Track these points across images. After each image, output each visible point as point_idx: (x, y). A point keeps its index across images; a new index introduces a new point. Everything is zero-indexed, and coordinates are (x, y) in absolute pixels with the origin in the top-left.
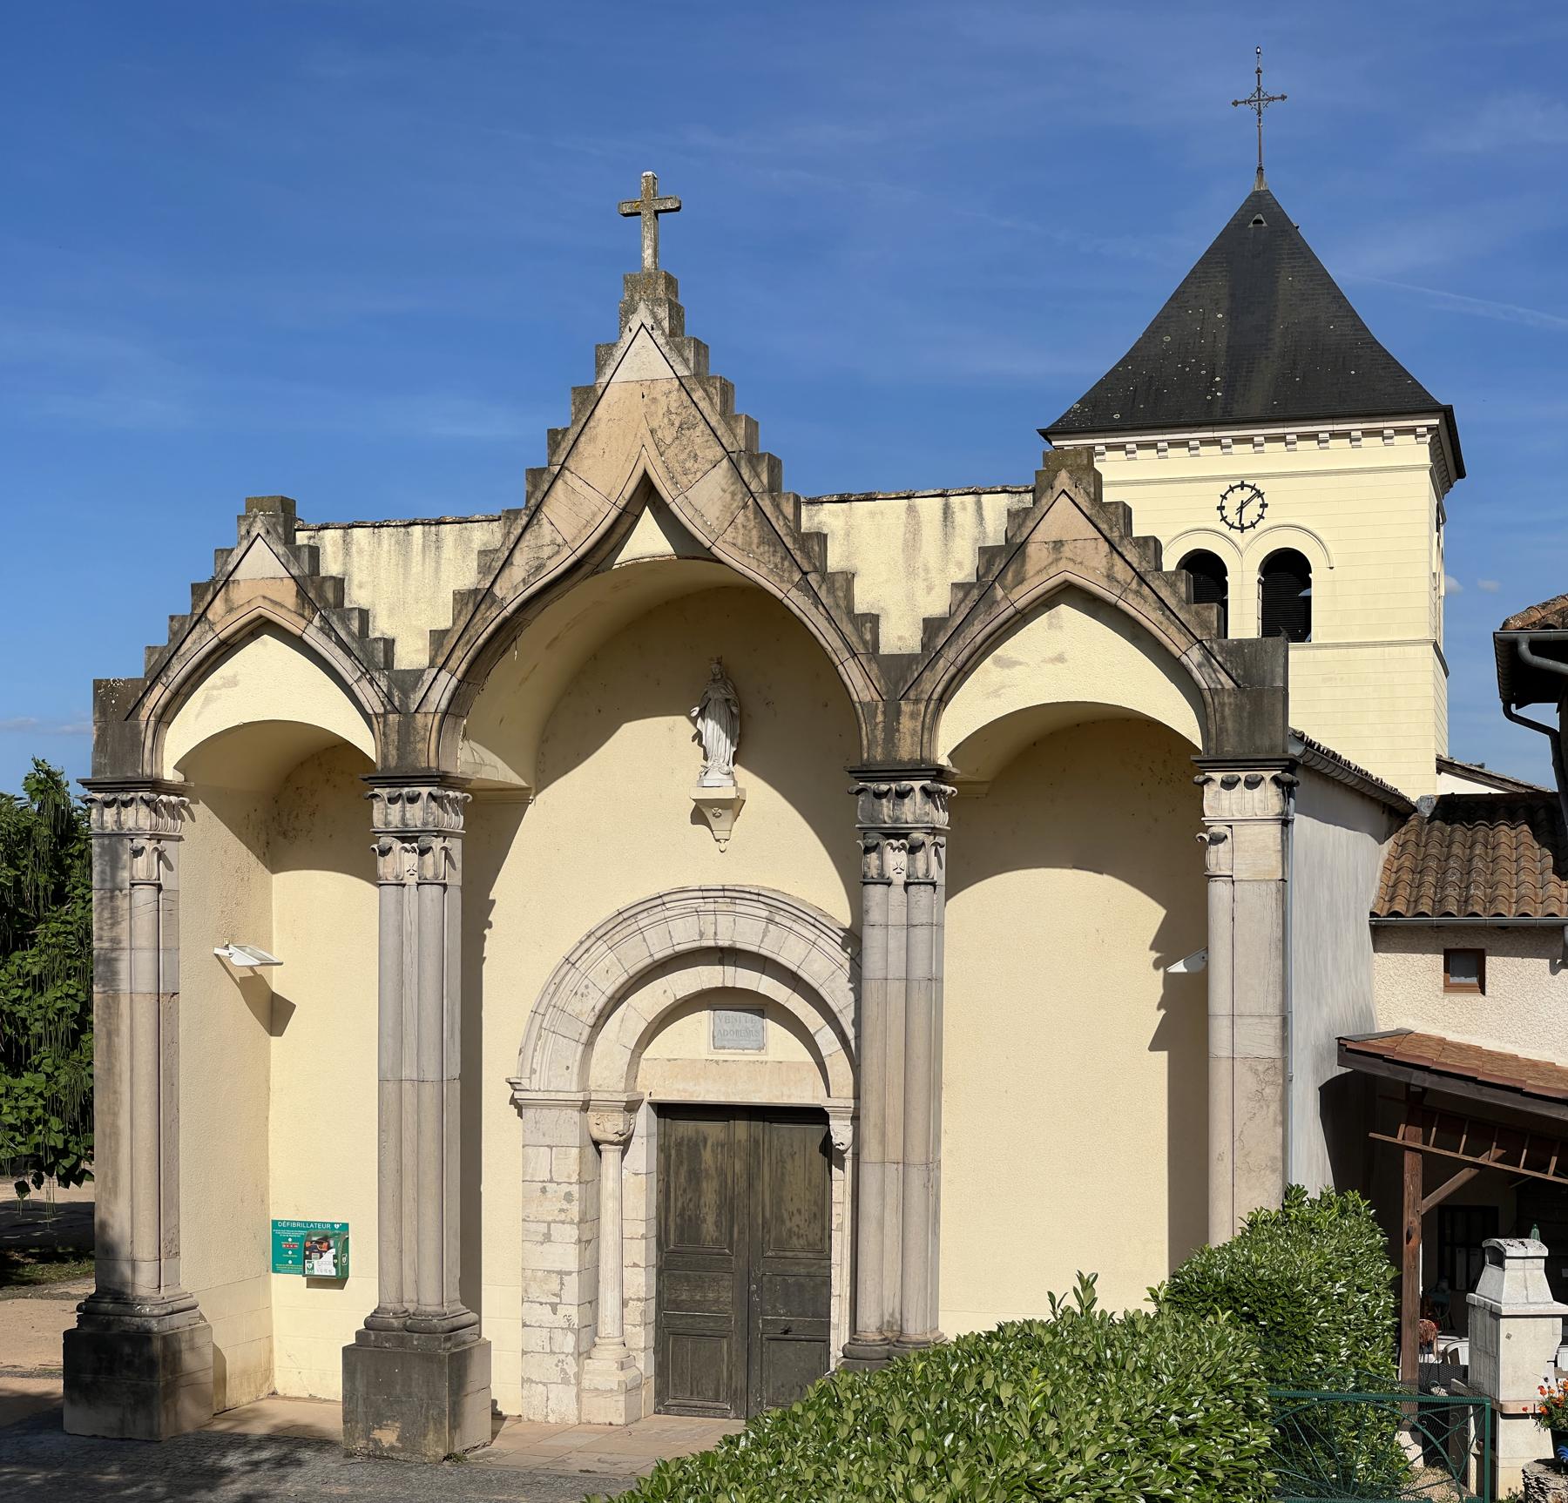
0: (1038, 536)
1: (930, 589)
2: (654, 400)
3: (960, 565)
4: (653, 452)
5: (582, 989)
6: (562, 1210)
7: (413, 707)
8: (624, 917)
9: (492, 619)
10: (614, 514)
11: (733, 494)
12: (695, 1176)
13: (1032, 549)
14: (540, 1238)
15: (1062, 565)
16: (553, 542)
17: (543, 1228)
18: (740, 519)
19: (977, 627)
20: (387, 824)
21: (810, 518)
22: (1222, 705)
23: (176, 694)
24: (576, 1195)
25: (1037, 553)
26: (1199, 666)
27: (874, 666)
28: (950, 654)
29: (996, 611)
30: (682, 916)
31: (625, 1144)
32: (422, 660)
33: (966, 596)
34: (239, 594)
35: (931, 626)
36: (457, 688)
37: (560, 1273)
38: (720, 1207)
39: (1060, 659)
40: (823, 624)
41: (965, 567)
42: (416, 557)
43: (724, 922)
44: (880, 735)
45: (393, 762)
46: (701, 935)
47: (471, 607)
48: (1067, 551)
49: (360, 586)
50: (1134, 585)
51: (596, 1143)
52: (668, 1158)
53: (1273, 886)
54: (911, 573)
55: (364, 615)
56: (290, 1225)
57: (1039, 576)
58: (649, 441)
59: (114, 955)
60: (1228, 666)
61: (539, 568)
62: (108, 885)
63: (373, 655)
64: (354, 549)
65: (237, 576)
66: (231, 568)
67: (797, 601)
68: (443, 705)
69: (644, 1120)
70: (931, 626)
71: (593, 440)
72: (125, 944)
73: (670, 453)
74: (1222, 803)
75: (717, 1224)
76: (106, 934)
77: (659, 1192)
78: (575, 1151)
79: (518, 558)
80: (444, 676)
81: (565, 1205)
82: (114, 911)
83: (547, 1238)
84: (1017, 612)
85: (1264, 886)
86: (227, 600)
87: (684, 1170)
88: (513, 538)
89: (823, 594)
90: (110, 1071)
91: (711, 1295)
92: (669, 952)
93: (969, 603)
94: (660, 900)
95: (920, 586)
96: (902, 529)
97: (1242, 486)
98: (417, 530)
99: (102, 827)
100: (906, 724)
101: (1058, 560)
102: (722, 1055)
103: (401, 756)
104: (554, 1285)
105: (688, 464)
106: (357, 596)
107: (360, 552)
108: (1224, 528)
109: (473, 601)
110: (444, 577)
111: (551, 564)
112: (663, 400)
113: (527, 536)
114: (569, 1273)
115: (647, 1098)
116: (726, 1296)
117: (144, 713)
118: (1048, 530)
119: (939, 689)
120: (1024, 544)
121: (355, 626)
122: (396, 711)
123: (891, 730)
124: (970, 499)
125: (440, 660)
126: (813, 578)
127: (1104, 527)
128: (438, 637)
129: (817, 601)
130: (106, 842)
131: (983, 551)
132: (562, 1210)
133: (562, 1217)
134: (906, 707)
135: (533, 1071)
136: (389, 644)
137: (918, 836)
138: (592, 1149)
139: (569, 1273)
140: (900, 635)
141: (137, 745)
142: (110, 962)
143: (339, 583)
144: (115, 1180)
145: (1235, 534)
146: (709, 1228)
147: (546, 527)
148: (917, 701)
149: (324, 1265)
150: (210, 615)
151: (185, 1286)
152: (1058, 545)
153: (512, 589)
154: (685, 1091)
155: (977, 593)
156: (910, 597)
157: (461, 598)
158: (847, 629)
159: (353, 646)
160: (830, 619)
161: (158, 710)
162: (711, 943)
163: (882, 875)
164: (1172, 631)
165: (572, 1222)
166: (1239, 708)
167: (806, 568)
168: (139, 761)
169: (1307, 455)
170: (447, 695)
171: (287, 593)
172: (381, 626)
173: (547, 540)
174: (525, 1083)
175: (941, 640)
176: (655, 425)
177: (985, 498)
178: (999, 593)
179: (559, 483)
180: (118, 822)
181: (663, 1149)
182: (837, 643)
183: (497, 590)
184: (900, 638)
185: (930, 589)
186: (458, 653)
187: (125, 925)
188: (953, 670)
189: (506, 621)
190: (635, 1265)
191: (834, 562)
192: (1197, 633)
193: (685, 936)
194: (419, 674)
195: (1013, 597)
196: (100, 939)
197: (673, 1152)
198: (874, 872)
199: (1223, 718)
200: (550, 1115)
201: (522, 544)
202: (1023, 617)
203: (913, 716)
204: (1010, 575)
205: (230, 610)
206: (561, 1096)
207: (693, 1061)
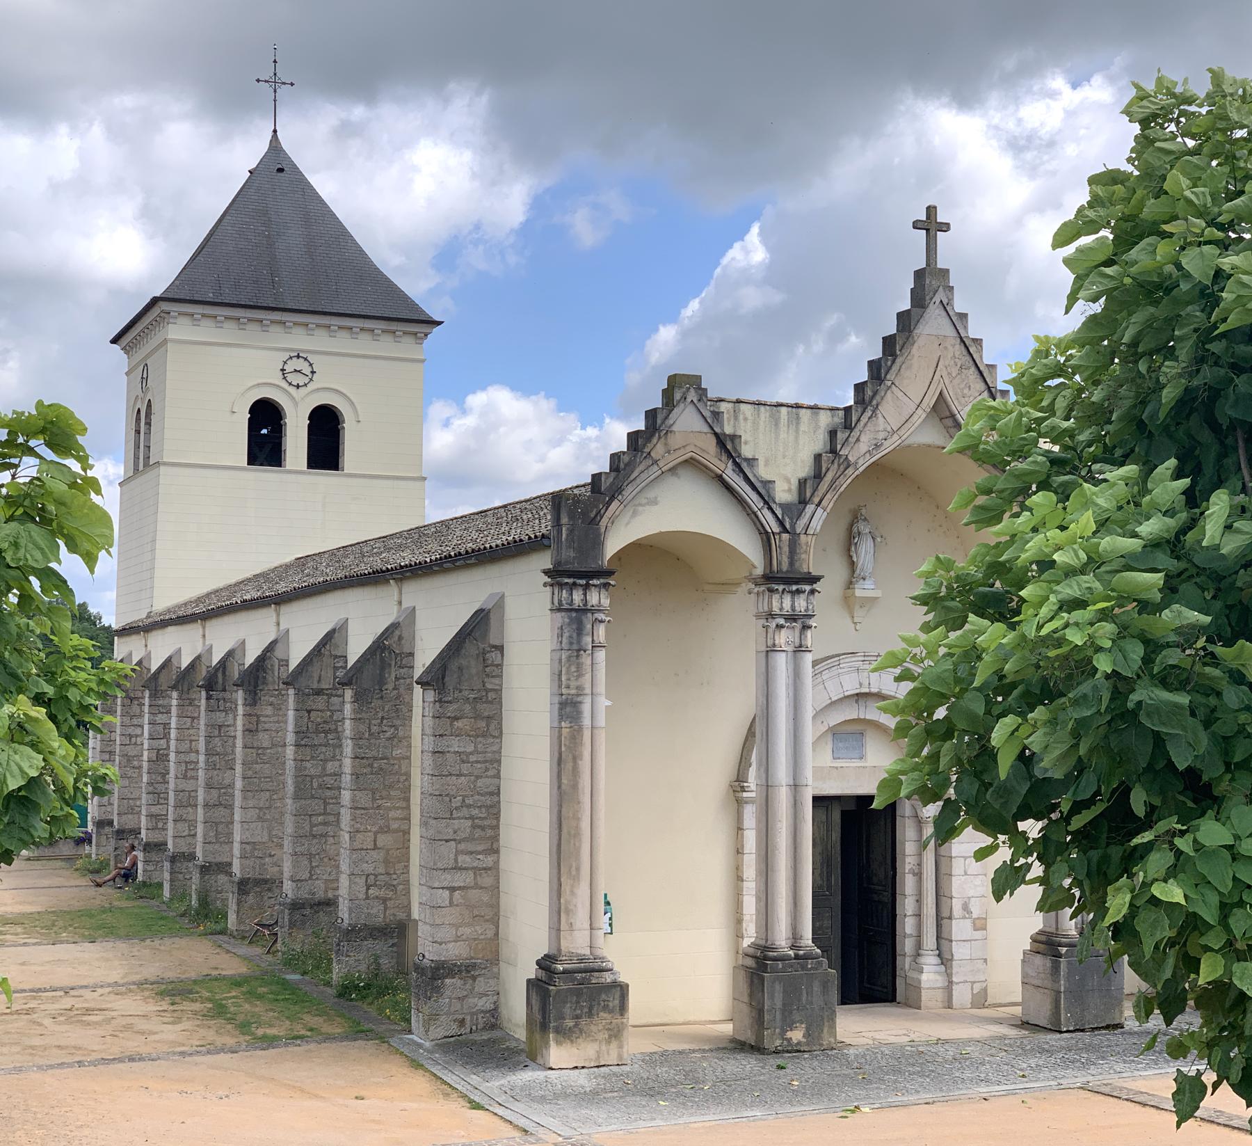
20: (781, 609)
45: (785, 567)
46: (861, 684)
59: (579, 699)
61: (877, 446)
62: (575, 647)
64: (741, 417)
71: (910, 367)
72: (588, 691)
73: (956, 381)
76: (573, 684)
80: (820, 510)
86: (666, 444)
98: (784, 410)
99: (571, 603)
102: (838, 764)
103: (791, 563)
105: (966, 391)
107: (746, 419)
110: (801, 442)
112: (950, 348)
122: (785, 530)
125: (816, 500)
130: (574, 615)
144: (578, 869)
147: (881, 419)
159: (758, 485)
162: (867, 690)
169: (342, 342)
171: (710, 444)
173: (881, 428)
180: (585, 602)
186: (829, 496)
187: (588, 676)
196: (568, 687)
207: (823, 768)
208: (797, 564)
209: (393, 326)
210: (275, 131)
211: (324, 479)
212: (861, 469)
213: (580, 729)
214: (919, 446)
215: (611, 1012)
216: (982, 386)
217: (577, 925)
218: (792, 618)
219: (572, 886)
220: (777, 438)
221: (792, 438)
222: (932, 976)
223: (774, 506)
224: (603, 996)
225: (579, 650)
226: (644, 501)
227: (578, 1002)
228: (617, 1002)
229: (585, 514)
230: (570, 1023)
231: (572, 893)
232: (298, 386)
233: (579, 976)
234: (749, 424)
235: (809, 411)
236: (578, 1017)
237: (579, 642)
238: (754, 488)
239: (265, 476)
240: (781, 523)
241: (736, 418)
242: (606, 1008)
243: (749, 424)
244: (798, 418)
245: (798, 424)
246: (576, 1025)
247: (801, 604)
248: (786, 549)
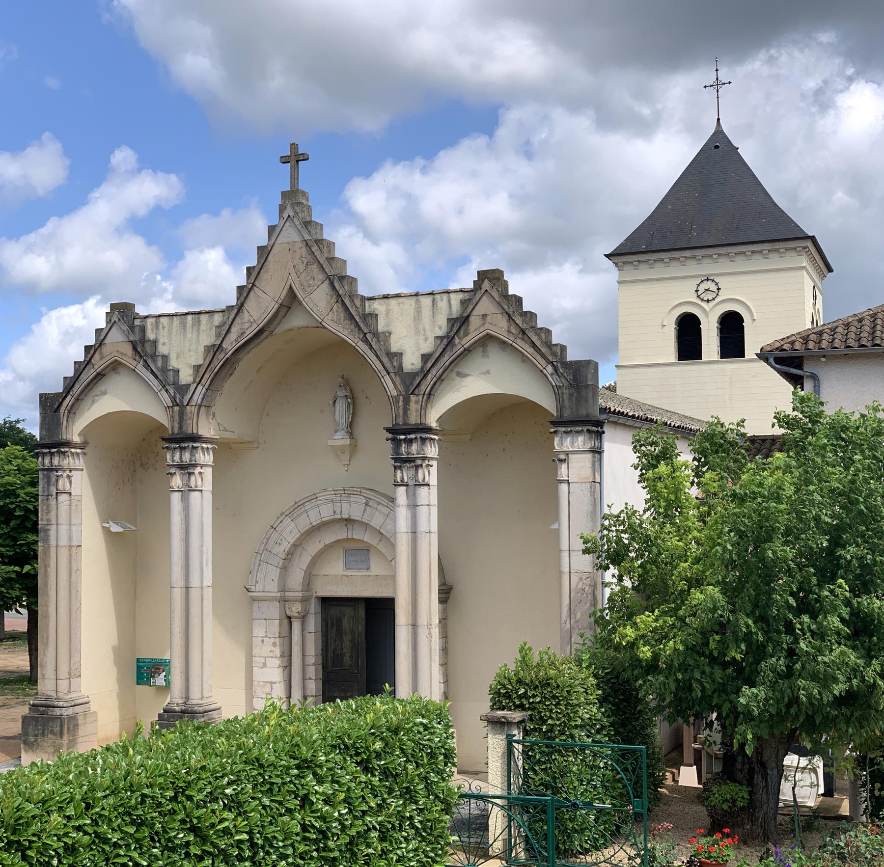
0: (475, 312)
1: (426, 339)
2: (295, 251)
3: (440, 327)
4: (294, 275)
5: (279, 541)
6: (271, 651)
7: (185, 403)
8: (298, 505)
9: (221, 357)
10: (276, 307)
11: (332, 296)
12: (340, 633)
13: (472, 319)
14: (261, 665)
15: (487, 326)
16: (249, 321)
17: (263, 660)
18: (335, 308)
19: (446, 357)
21: (370, 306)
22: (563, 394)
23: (77, 400)
24: (278, 643)
25: (474, 321)
26: (552, 375)
27: (398, 378)
28: (434, 371)
29: (455, 349)
30: (325, 504)
31: (303, 618)
32: (190, 379)
33: (442, 341)
34: (106, 350)
35: (425, 358)
36: (205, 393)
37: (271, 683)
40: (374, 358)
41: (441, 327)
42: (189, 329)
43: (345, 505)
44: (401, 411)
45: (176, 431)
46: (334, 512)
47: (211, 354)
48: (488, 319)
49: (164, 344)
50: (520, 336)
51: (289, 618)
52: (327, 625)
53: (588, 485)
54: (417, 332)
55: (165, 358)
56: (145, 661)
57: (475, 330)
58: (292, 271)
60: (565, 374)
61: (242, 334)
62: (46, 493)
63: (165, 376)
65: (106, 341)
66: (102, 338)
67: (362, 347)
68: (199, 402)
69: (314, 607)
70: (425, 358)
71: (267, 271)
72: (54, 521)
73: (302, 277)
74: (563, 443)
76: (45, 518)
77: (323, 642)
78: (277, 622)
79: (233, 330)
81: (273, 649)
82: (48, 506)
83: (265, 665)
84: (465, 349)
85: (584, 485)
87: (334, 630)
88: (231, 319)
89: (373, 344)
90: (46, 585)
92: (320, 521)
93: (443, 346)
94: (314, 497)
95: (422, 338)
96: (413, 311)
97: (708, 280)
98: (190, 317)
99: (43, 465)
100: (413, 407)
101: (484, 324)
102: (349, 573)
103: (180, 428)
104: (268, 690)
105: (311, 282)
106: (162, 349)
107: (163, 327)
108: (699, 302)
109: (214, 350)
110: (201, 338)
111: (248, 332)
112: (299, 251)
113: (237, 318)
114: (275, 683)
115: (315, 595)
117: (63, 409)
118: (480, 309)
119: (429, 389)
120: (468, 316)
121: (159, 363)
122: (178, 405)
123: (406, 410)
124: (445, 296)
125: (198, 380)
126: (369, 336)
127: (505, 307)
128: (197, 368)
129: (371, 347)
131: (449, 320)
132: (271, 651)
133: (271, 654)
134: (413, 398)
135: (257, 582)
136: (177, 372)
137: (419, 462)
138: (286, 621)
139: (275, 683)
140: (411, 362)
141: (58, 424)
142: (46, 531)
143: (155, 342)
144: (47, 639)
145: (704, 304)
146: (347, 660)
148: (418, 395)
149: (160, 680)
150: (93, 361)
151: (84, 691)
152: (484, 316)
153: (230, 344)
155: (447, 341)
156: (417, 344)
157: (207, 349)
158: (385, 360)
159: (158, 374)
160: (377, 356)
161: (69, 408)
162: (339, 517)
163: (402, 481)
164: (539, 357)
165: (276, 657)
166: (571, 395)
167: (366, 331)
168: (58, 434)
170: (201, 396)
171: (128, 350)
172: (174, 363)
173: (246, 320)
174: (253, 588)
175: (429, 365)
176: (295, 263)
177: (452, 295)
178: (457, 340)
179: (252, 292)
181: (325, 621)
182: (381, 367)
183: (224, 345)
184: (412, 364)
185: (426, 339)
186: (206, 376)
187: (53, 513)
188: (435, 379)
189: (228, 359)
190: (310, 679)
191: (381, 328)
192: (550, 358)
193: (326, 512)
194: (188, 386)
195: (463, 342)
198: (399, 480)
199: (563, 400)
200: (265, 605)
201: (236, 322)
202: (468, 351)
203: (416, 402)
204: (462, 331)
205: (102, 358)
206: (269, 594)
207: (336, 576)
208: (184, 428)
209: (777, 245)
210: (719, 120)
211: (733, 366)
212: (230, 353)
213: (49, 546)
214: (299, 328)
215: (55, 735)
216: (321, 277)
217: (47, 676)
218: (182, 467)
219: (44, 650)
220: (185, 336)
221: (195, 336)
223: (168, 387)
224: (51, 724)
225: (48, 496)
226: (99, 393)
227: (36, 726)
228: (58, 728)
229: (51, 406)
230: (32, 739)
231: (44, 654)
232: (708, 301)
233: (42, 709)
234: (166, 330)
235: (207, 316)
236: (36, 736)
237: (48, 490)
238: (156, 377)
239: (690, 368)
240: (173, 399)
241: (157, 328)
242: (52, 732)
243: (166, 330)
244: (199, 321)
245: (199, 325)
246: (36, 741)
247: (187, 457)
248: (177, 418)
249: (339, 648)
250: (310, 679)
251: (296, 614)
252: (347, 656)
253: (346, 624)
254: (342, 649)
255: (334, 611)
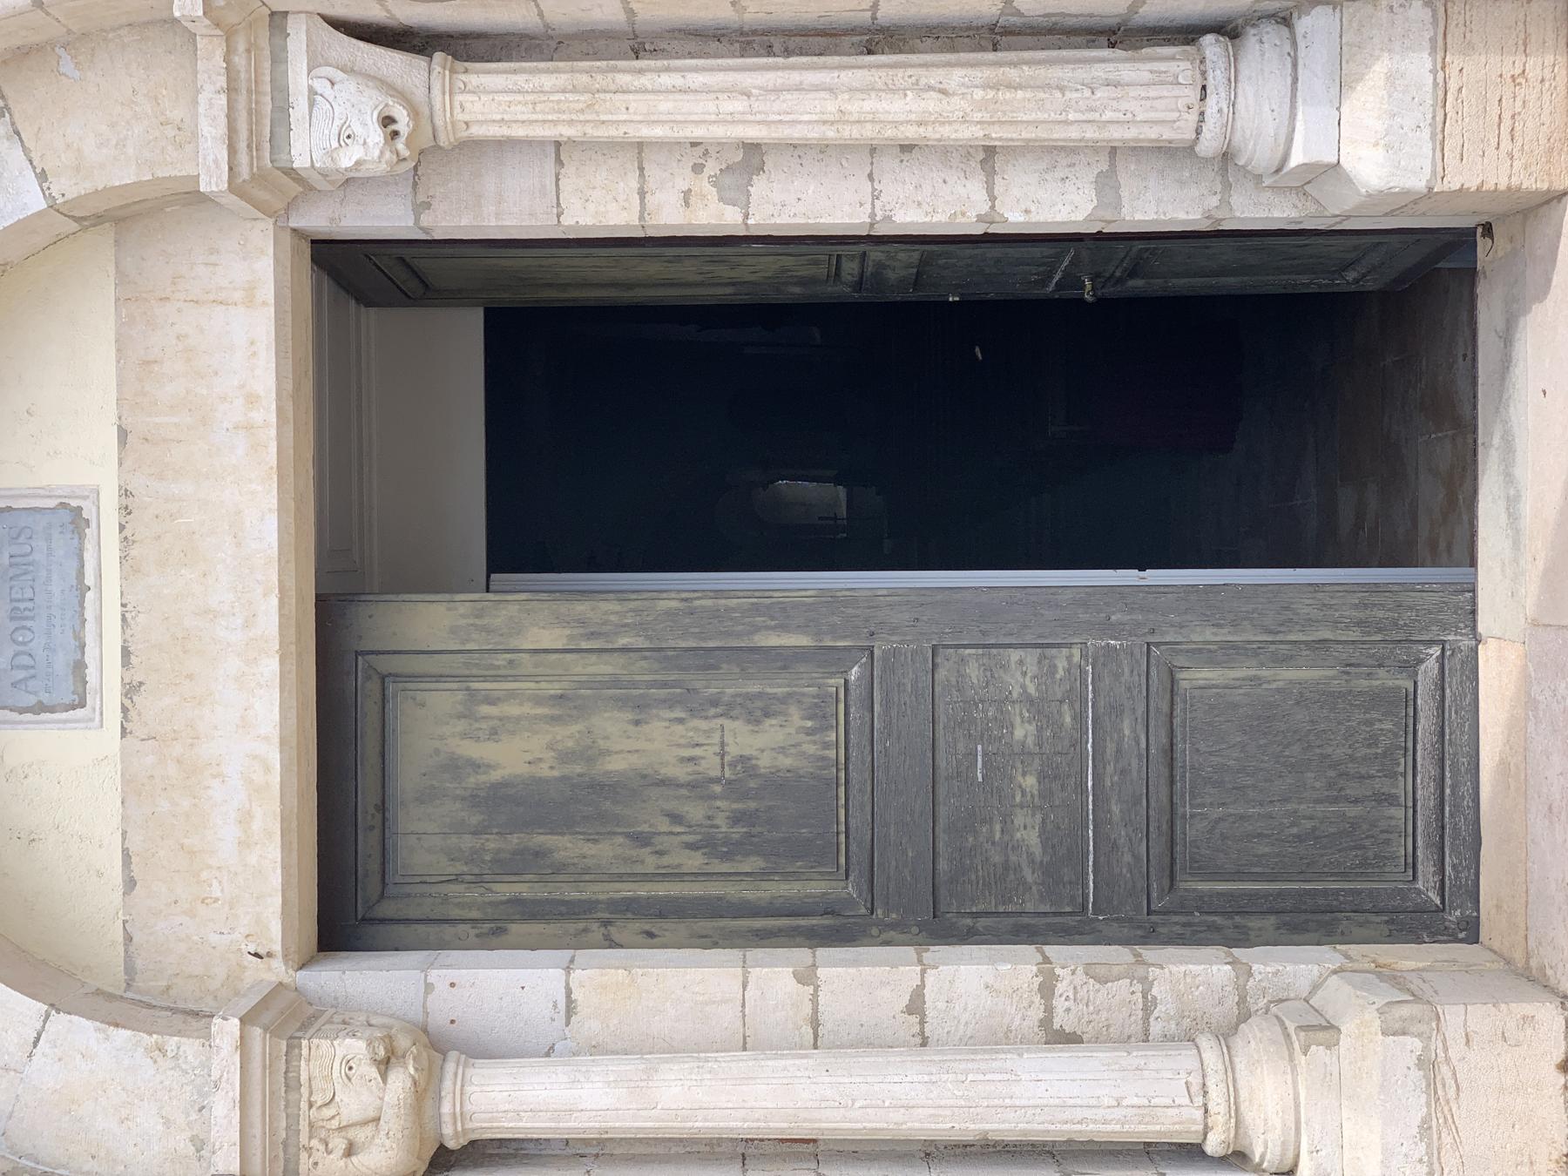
12: (588, 800)
31: (434, 1048)
38: (697, 705)
39: (452, 985)
52: (532, 911)
69: (374, 981)
75: (758, 711)
77: (650, 939)
87: (566, 846)
91: (1023, 731)
102: (106, 676)
115: (278, 971)
116: (1021, 673)
146: (775, 743)
154: (245, 818)
181: (494, 929)
190: (916, 1006)
197: (505, 890)
207: (132, 788)
222: (1367, 107)
249: (695, 812)
250: (916, 1006)
251: (400, 1082)
252: (743, 739)
253: (519, 753)
254: (698, 787)
255: (426, 839)
